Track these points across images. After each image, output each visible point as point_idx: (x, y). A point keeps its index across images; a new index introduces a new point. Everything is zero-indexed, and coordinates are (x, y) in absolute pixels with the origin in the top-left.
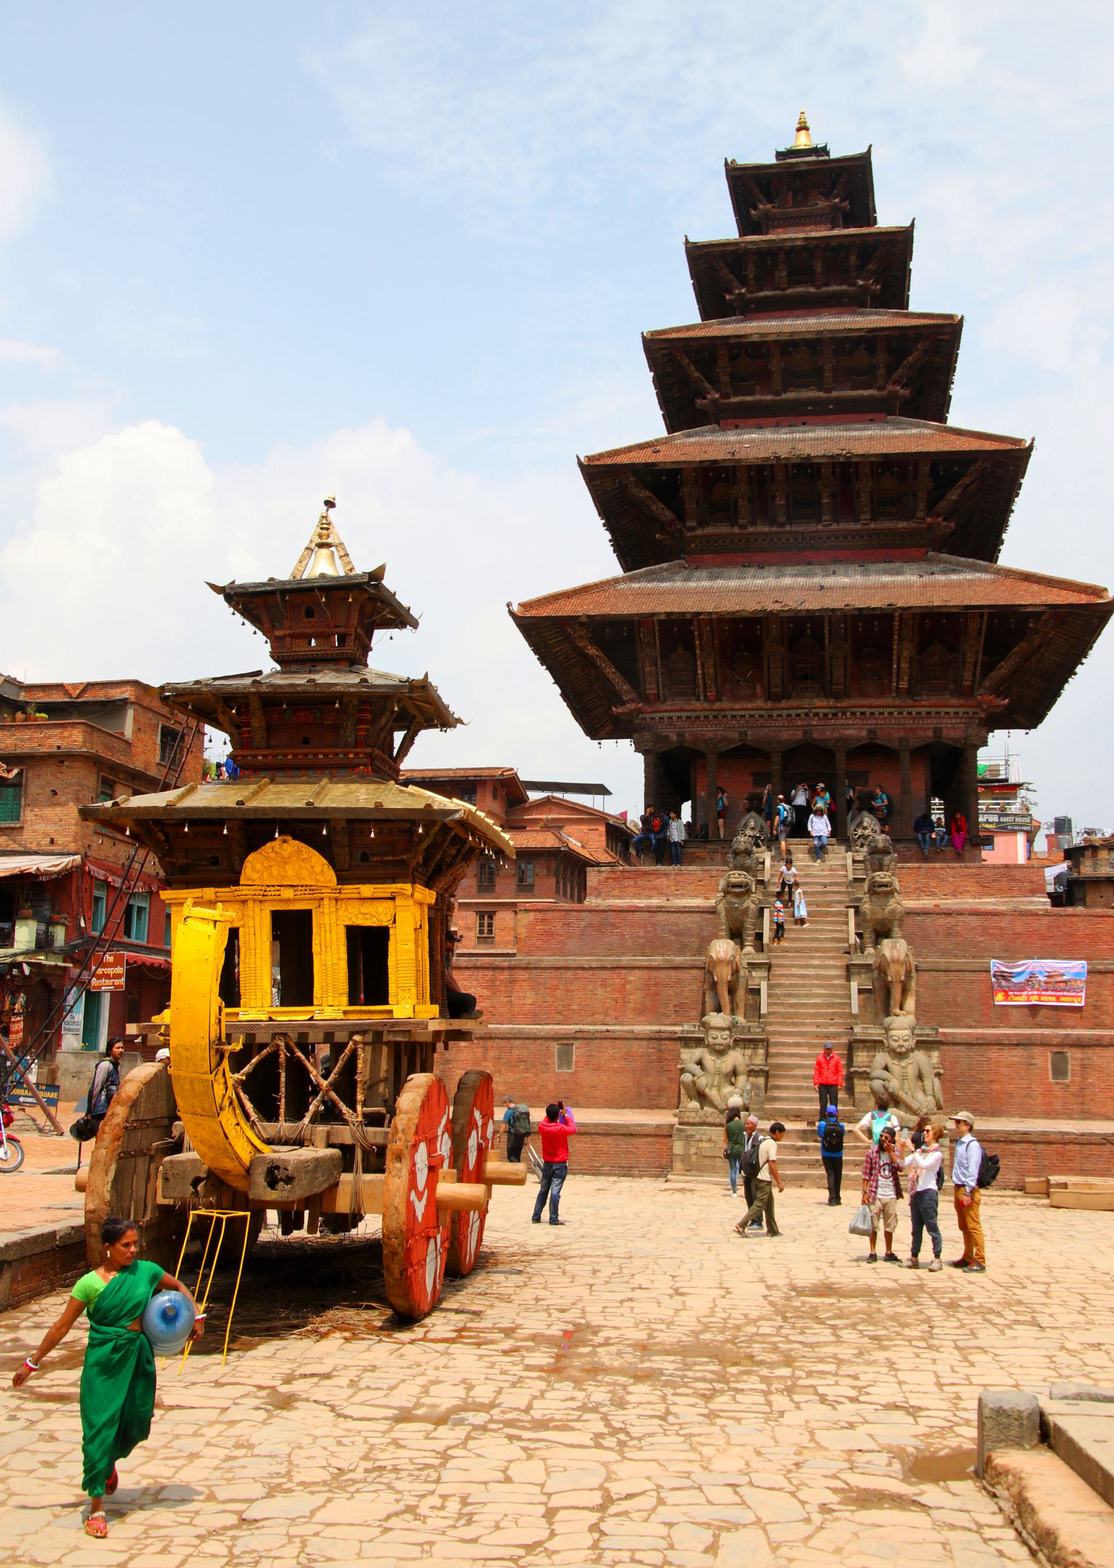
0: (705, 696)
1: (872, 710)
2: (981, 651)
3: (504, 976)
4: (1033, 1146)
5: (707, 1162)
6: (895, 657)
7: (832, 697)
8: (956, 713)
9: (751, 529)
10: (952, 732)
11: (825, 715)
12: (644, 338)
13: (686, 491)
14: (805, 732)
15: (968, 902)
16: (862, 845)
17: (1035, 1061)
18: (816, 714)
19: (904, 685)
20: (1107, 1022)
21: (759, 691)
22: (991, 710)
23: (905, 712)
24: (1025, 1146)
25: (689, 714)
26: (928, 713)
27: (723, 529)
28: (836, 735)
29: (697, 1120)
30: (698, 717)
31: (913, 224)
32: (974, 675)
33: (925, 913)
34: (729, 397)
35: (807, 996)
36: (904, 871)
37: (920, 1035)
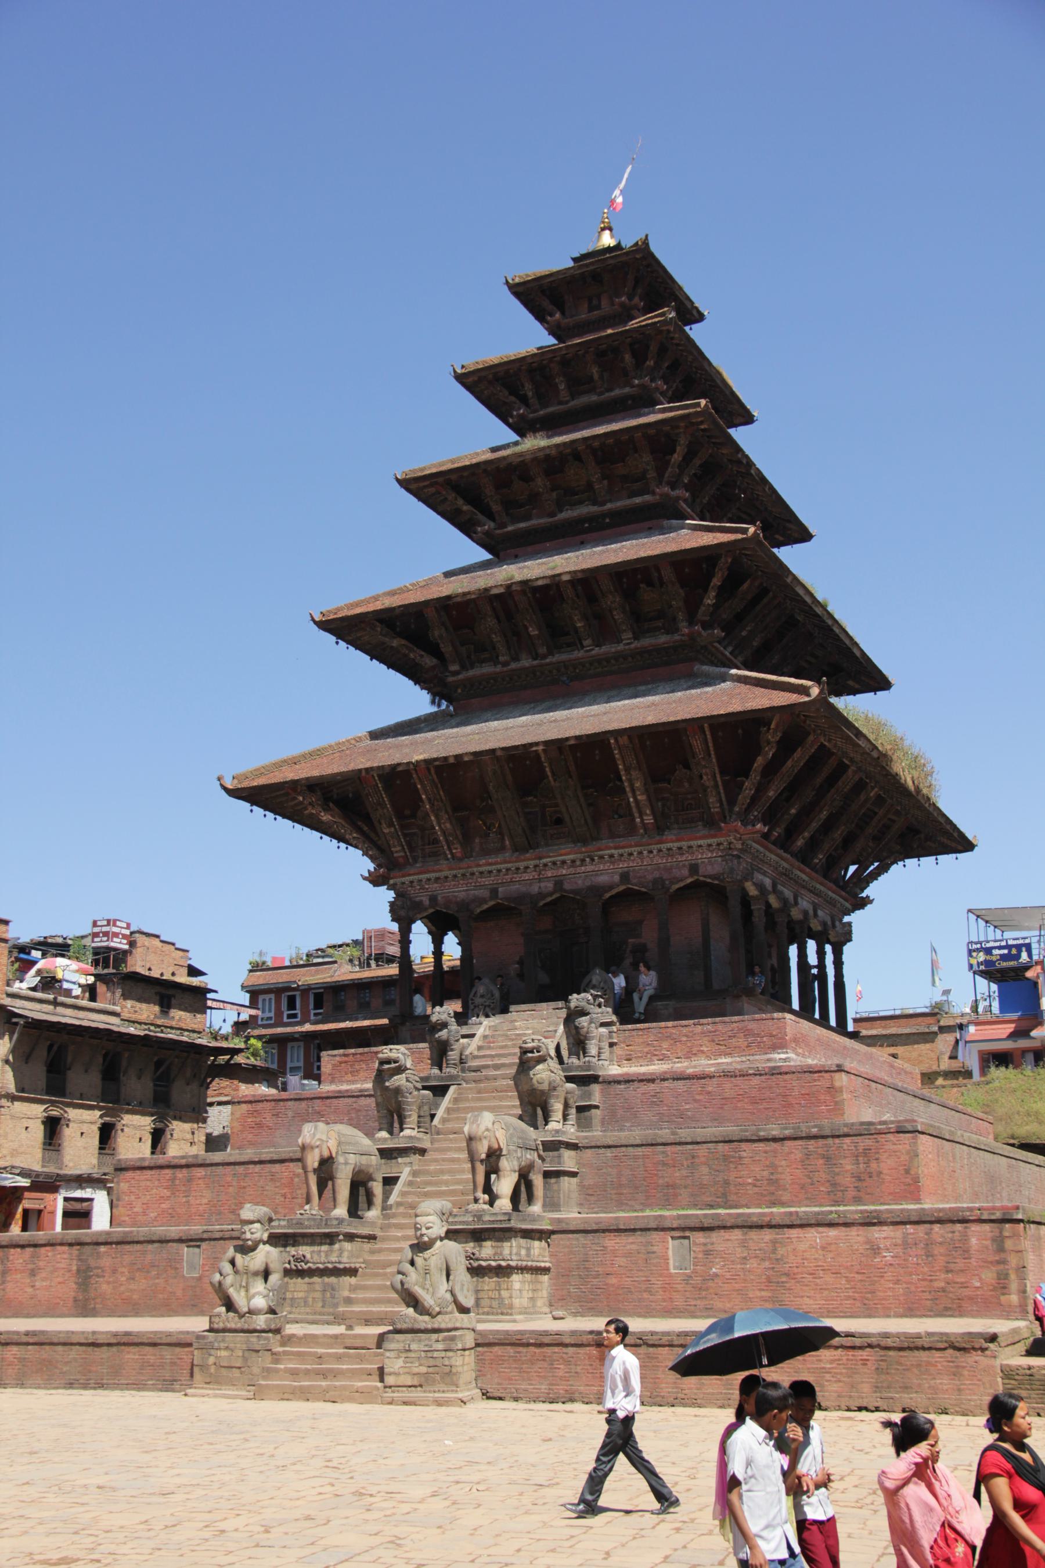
2: (717, 771)
3: (181, 1174)
4: (565, 1350)
5: (224, 1371)
6: (628, 789)
7: (579, 841)
8: (710, 845)
9: (513, 665)
10: (709, 868)
11: (573, 861)
13: (436, 633)
15: (704, 1064)
17: (655, 1249)
18: (564, 862)
19: (649, 819)
20: (784, 1198)
24: (556, 1349)
25: (437, 875)
26: (680, 848)
27: (487, 669)
28: (588, 883)
29: (221, 1325)
30: (446, 877)
33: (628, 1080)
34: (503, 525)
35: (446, 1183)
36: (634, 1033)
37: (453, 1223)
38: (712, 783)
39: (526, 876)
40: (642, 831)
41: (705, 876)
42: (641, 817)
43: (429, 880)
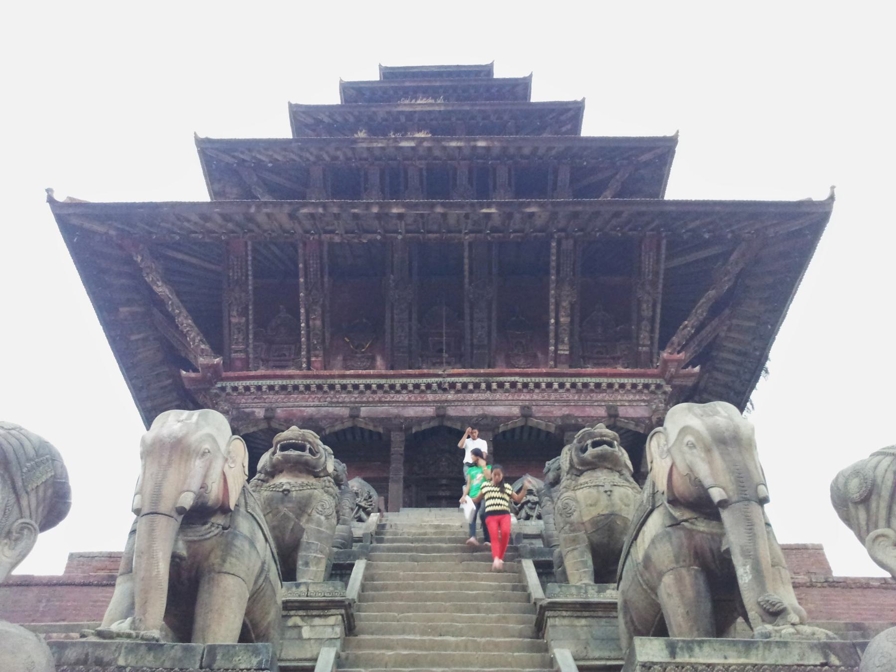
0: (309, 363)
1: (525, 380)
2: (660, 301)
6: (552, 307)
8: (634, 386)
11: (465, 385)
12: (290, 105)
14: (438, 408)
16: (528, 517)
18: (453, 386)
19: (564, 350)
21: (379, 361)
22: (677, 382)
23: (568, 382)
25: (284, 382)
26: (598, 385)
28: (481, 412)
30: (296, 387)
31: (531, 76)
32: (652, 338)
38: (651, 313)
39: (400, 397)
40: (552, 363)
41: (626, 418)
42: (556, 346)
43: (271, 388)
